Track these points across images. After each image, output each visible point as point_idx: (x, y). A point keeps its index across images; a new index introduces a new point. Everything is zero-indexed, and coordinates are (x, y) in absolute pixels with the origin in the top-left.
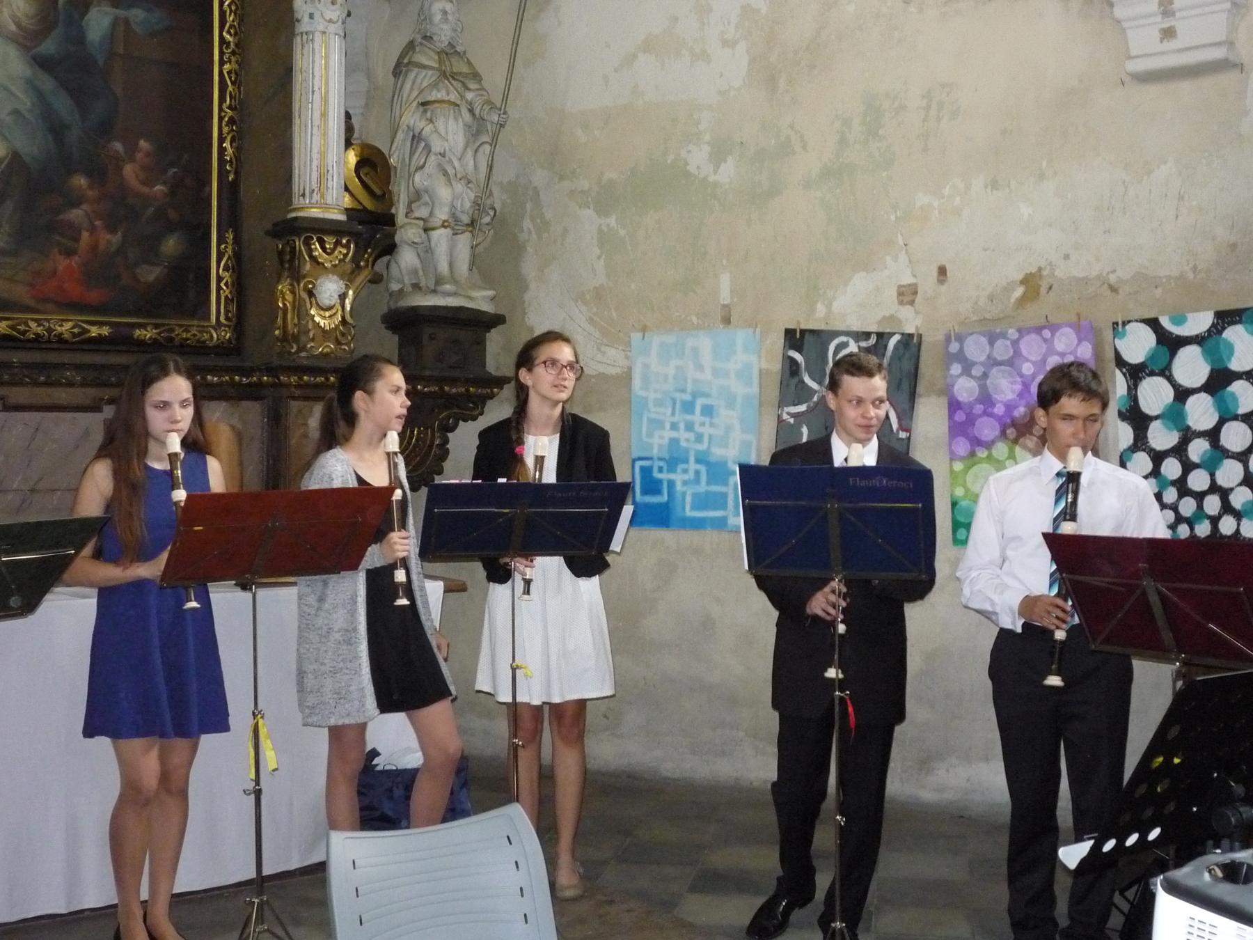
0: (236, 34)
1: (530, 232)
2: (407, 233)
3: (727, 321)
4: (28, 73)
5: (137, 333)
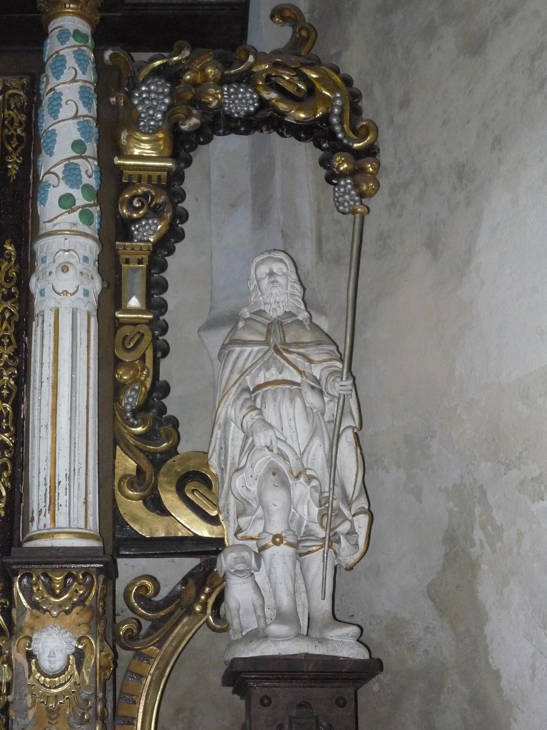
1: (482, 546)
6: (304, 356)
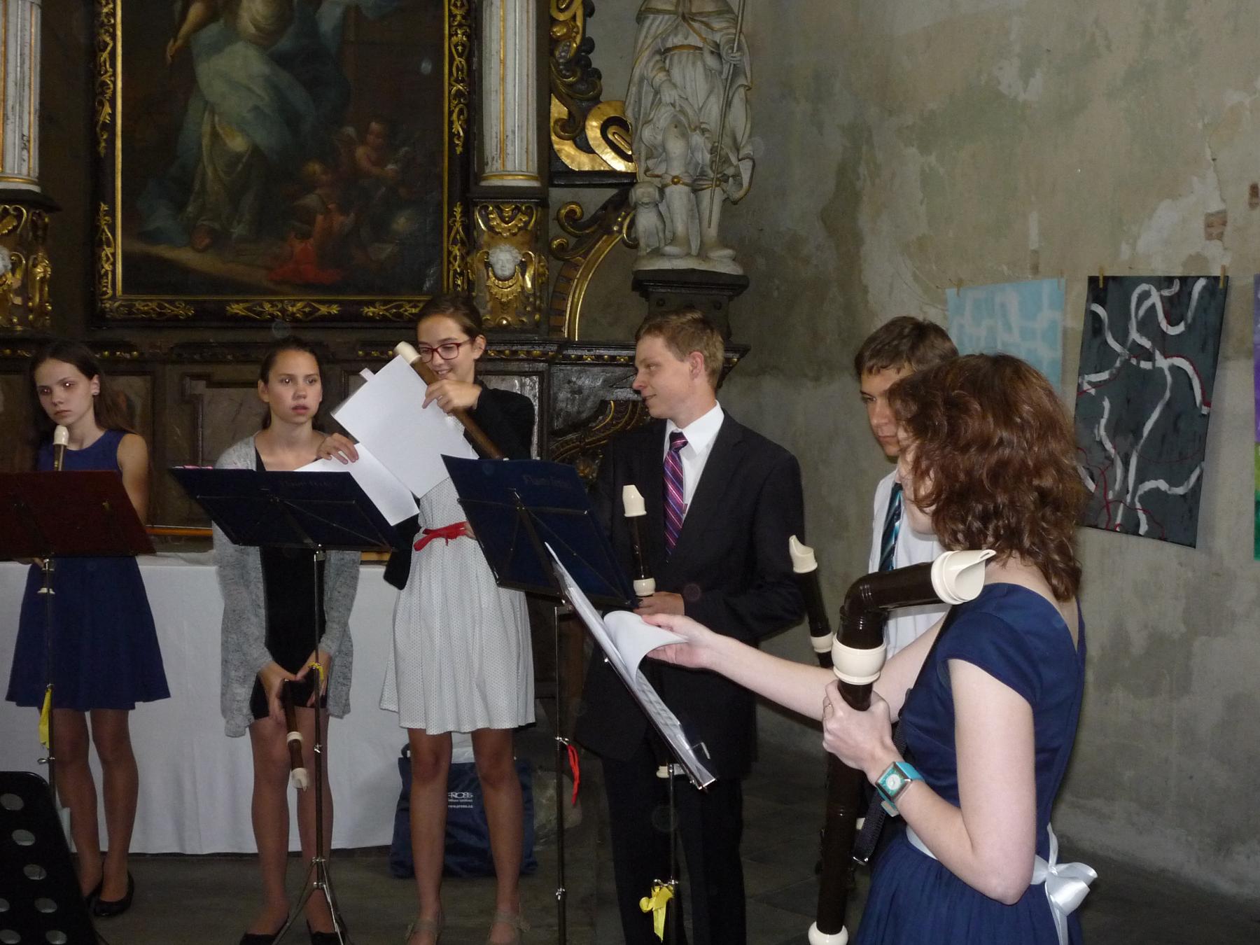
0: (462, 5)
2: (639, 193)
3: (1035, 269)
4: (266, 70)
5: (370, 311)
6: (707, 25)
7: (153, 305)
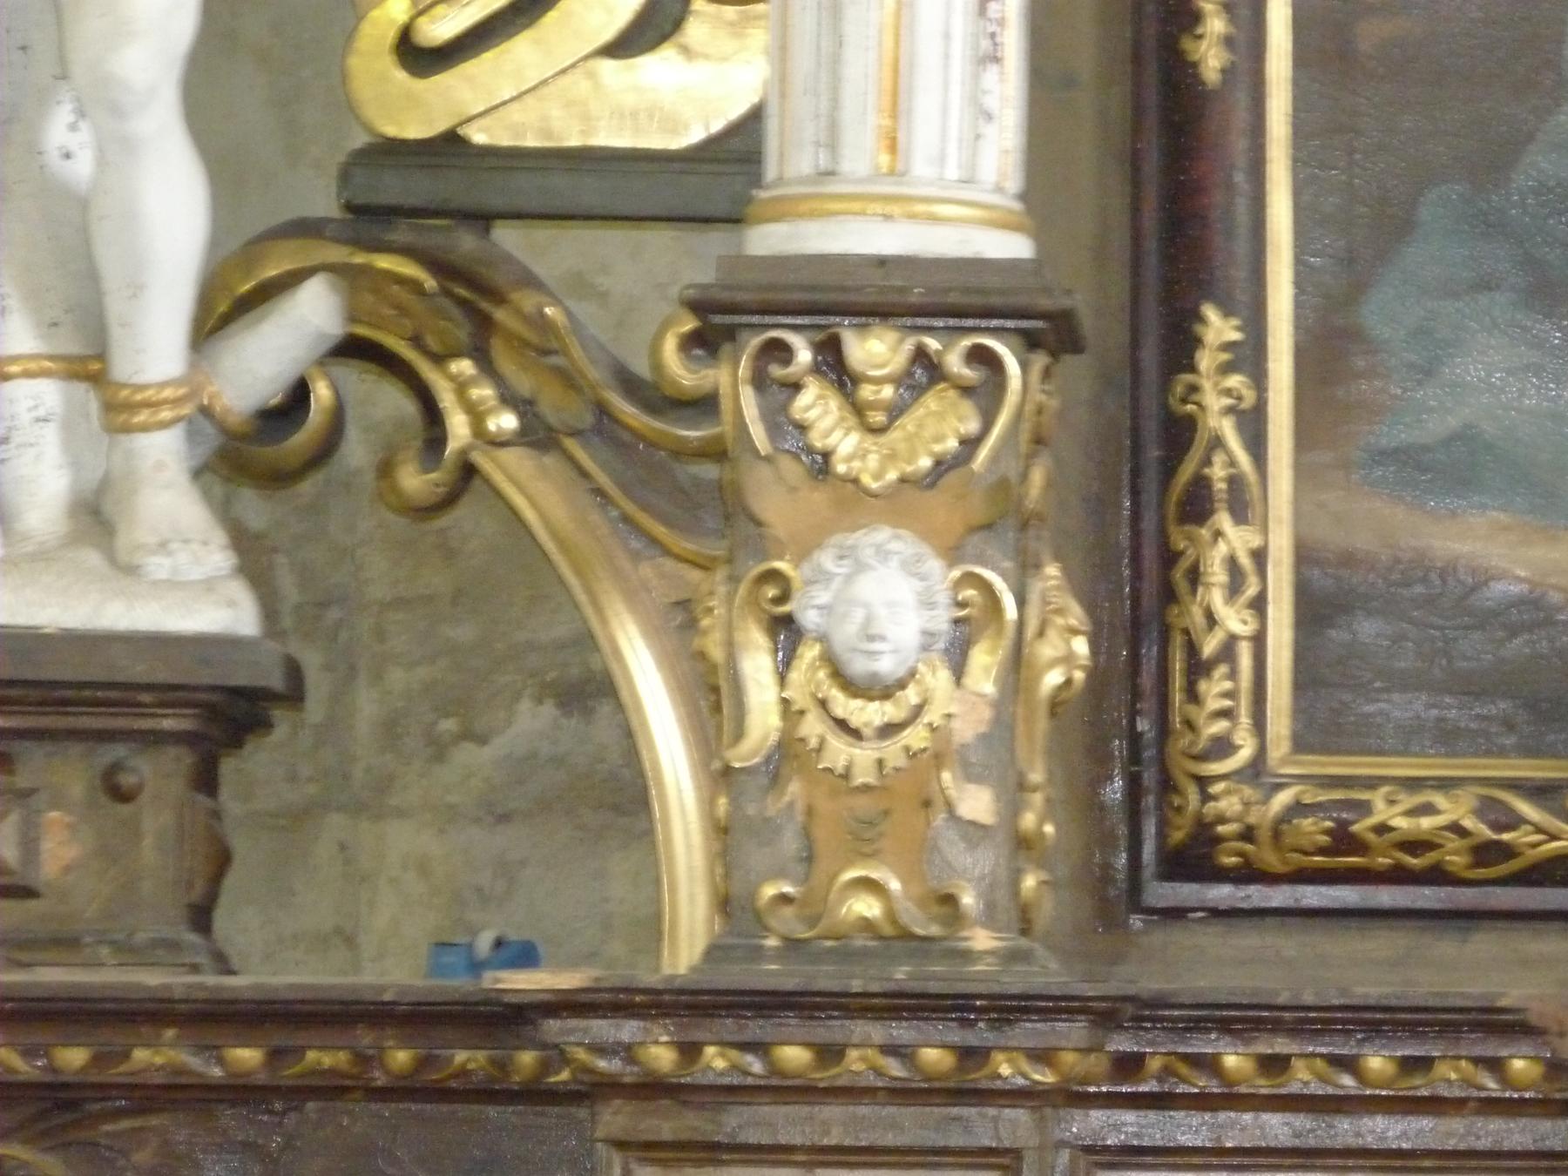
7: (1454, 809)
